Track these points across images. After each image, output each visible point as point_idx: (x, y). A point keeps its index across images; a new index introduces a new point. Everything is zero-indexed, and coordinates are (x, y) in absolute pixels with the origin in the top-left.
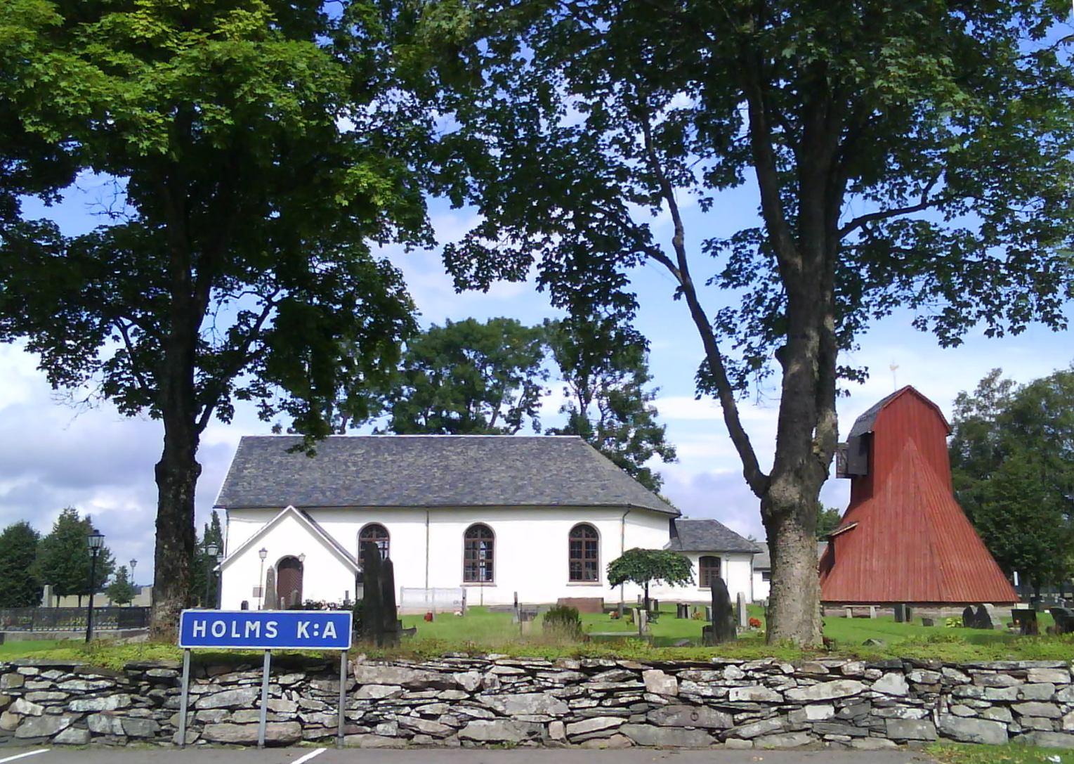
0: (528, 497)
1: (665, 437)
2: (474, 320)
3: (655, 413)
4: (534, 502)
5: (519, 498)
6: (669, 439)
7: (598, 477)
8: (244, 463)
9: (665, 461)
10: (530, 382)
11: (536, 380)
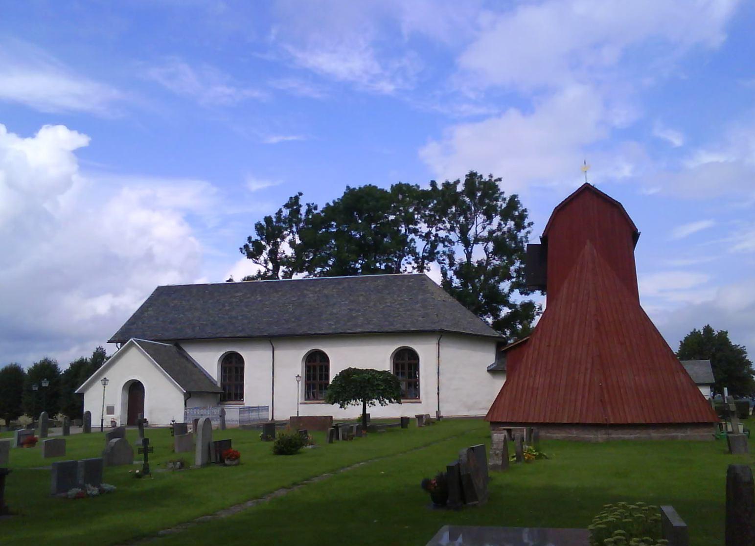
4: (359, 330)
10: (436, 235)
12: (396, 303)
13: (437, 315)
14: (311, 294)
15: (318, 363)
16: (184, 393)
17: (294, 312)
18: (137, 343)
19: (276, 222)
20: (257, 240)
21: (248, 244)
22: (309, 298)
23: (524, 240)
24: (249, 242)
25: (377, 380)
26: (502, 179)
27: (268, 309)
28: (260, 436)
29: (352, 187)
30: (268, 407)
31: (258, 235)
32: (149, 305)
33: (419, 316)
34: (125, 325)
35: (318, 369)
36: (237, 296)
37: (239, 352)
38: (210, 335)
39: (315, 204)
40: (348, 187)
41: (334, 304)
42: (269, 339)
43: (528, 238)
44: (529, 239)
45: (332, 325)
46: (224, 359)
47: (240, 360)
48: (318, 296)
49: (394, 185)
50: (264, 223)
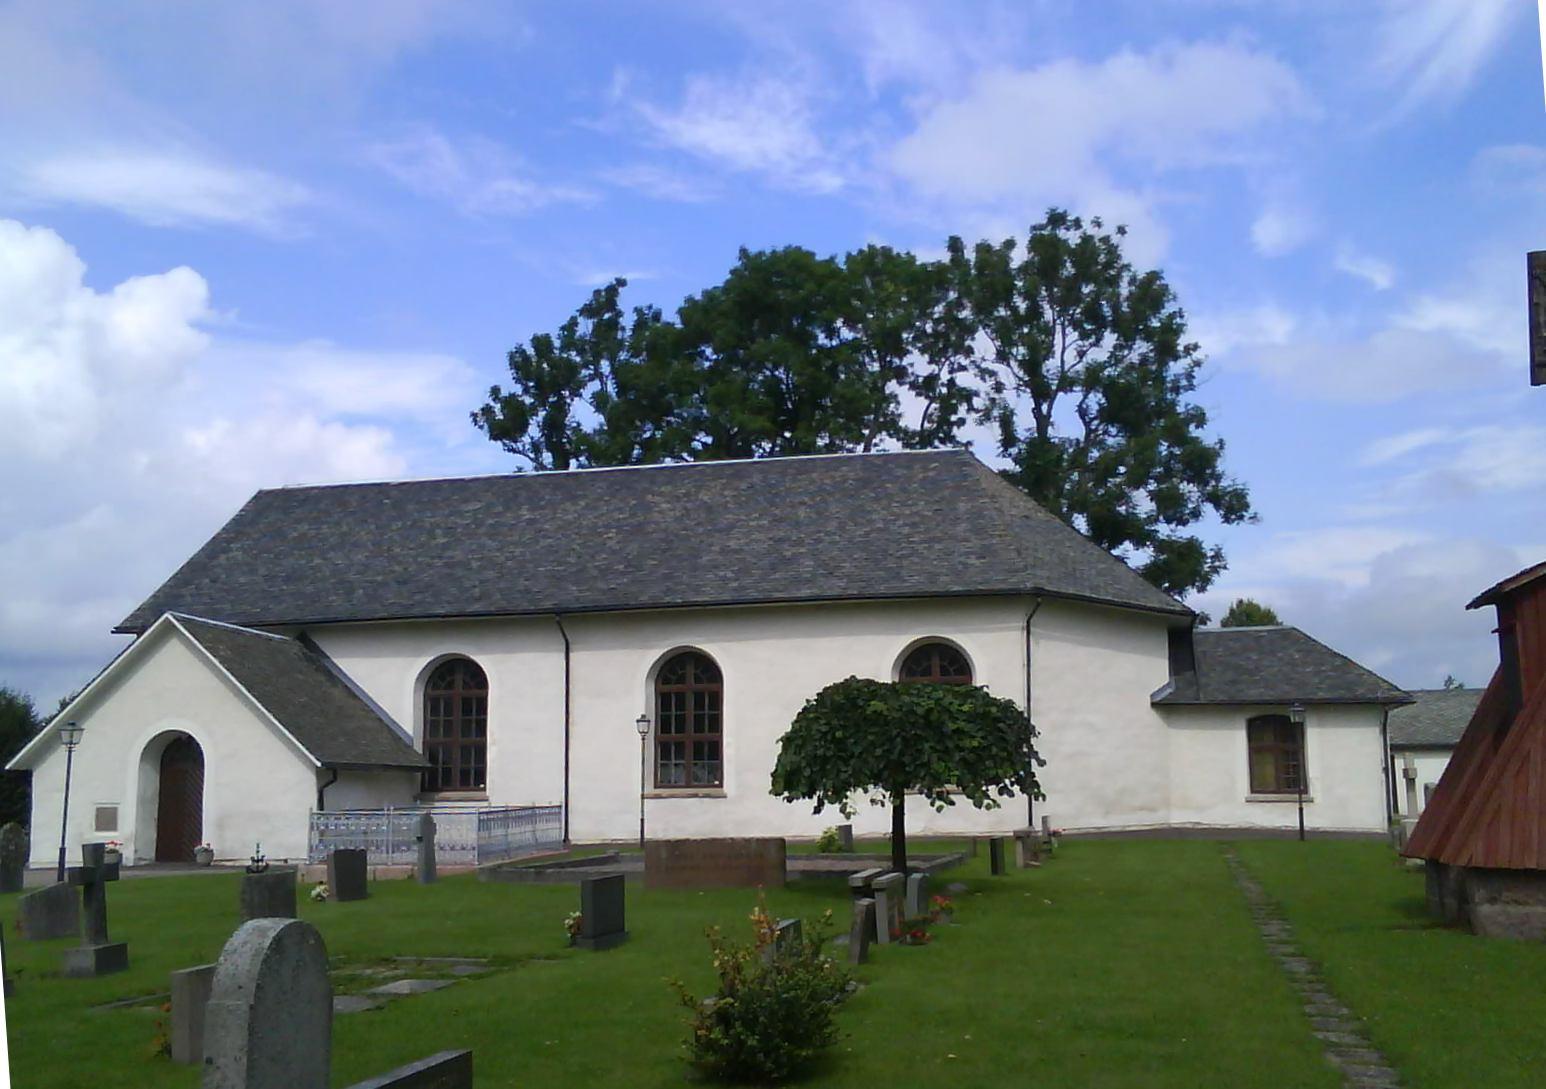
0: (798, 581)
1: (1221, 465)
2: (798, 249)
3: (1200, 418)
4: (805, 592)
5: (777, 585)
6: (1232, 470)
7: (978, 531)
9: (1227, 520)
10: (951, 383)
11: (965, 380)
14: (669, 502)
16: (317, 767)
19: (563, 349)
20: (513, 396)
21: (492, 404)
22: (660, 512)
23: (1184, 382)
24: (494, 400)
25: (955, 719)
27: (550, 540)
28: (571, 927)
29: (753, 250)
31: (517, 380)
32: (232, 535)
33: (967, 554)
34: (165, 586)
37: (472, 657)
38: (394, 611)
39: (654, 307)
40: (743, 252)
41: (731, 527)
42: (558, 618)
43: (1194, 377)
44: (1195, 382)
45: (729, 579)
46: (433, 673)
47: (477, 678)
48: (685, 509)
49: (854, 253)
50: (531, 351)
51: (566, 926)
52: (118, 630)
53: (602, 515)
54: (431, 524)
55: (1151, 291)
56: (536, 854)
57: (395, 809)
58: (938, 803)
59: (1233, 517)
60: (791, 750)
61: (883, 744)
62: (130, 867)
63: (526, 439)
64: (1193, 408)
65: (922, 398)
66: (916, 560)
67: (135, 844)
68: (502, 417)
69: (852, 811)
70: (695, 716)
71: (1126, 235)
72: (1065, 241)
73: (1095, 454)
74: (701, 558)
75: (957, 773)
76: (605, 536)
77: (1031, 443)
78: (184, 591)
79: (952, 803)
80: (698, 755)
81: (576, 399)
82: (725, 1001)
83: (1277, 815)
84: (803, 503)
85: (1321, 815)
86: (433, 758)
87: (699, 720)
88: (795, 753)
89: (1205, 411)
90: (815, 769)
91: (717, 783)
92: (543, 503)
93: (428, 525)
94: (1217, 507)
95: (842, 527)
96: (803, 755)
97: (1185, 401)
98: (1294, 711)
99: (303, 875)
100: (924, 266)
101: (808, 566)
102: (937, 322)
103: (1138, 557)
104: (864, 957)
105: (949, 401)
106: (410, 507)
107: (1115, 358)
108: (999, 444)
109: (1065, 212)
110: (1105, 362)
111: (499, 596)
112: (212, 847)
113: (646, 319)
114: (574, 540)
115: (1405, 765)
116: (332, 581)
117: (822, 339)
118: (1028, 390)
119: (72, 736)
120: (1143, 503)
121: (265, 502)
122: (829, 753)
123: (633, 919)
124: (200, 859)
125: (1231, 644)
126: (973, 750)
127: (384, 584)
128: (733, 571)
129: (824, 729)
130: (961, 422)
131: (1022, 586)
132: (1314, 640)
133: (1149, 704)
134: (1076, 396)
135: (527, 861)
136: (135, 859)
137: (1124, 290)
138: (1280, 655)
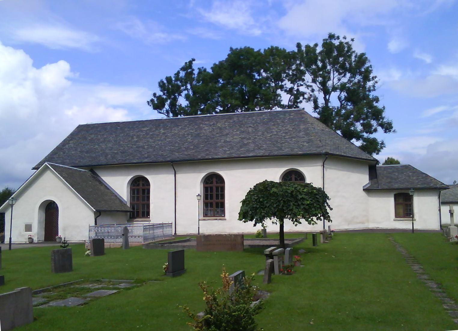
0: (248, 151)
1: (384, 115)
2: (249, 47)
4: (251, 155)
6: (387, 116)
7: (307, 134)
8: (71, 140)
9: (385, 132)
10: (298, 90)
11: (302, 89)
12: (282, 132)
13: (320, 141)
15: (214, 185)
16: (94, 211)
17: (192, 142)
18: (51, 166)
19: (175, 81)
20: (160, 96)
21: (154, 98)
23: (372, 88)
24: (154, 97)
26: (354, 39)
27: (170, 139)
28: (165, 268)
29: (234, 48)
30: (172, 223)
31: (161, 91)
32: (71, 139)
33: (304, 142)
35: (214, 189)
36: (144, 131)
37: (146, 176)
38: (120, 162)
39: (204, 68)
40: (231, 49)
41: (227, 134)
42: (172, 164)
43: (375, 87)
44: (376, 88)
45: (227, 150)
46: (133, 182)
47: (147, 183)
49: (267, 49)
50: (165, 82)
51: (163, 268)
52: (34, 169)
53: (186, 131)
54: (132, 134)
55: (362, 59)
56: (164, 239)
57: (116, 225)
58: (296, 223)
59: (388, 131)
60: (245, 206)
61: (276, 203)
62: (37, 243)
63: (164, 109)
64: (375, 97)
65: (289, 95)
66: (286, 144)
67: (37, 236)
68: (156, 102)
69: (266, 226)
70: (216, 194)
71: (354, 41)
72: (334, 44)
73: (343, 111)
74: (218, 144)
75: (302, 213)
76: (187, 138)
77: (323, 108)
78: (54, 156)
79: (301, 223)
80: (217, 206)
81: (180, 97)
82: (207, 316)
83: (404, 225)
84: (250, 127)
85: (419, 225)
86: (133, 208)
87: (217, 196)
88: (246, 206)
89: (379, 97)
90: (253, 212)
91: (223, 215)
92: (168, 128)
93: (131, 135)
94: (382, 128)
95: (263, 134)
96: (249, 207)
97: (372, 95)
98: (411, 191)
99: (87, 246)
100: (289, 52)
101: (252, 146)
102: (293, 71)
103: (358, 143)
104: (270, 281)
105: (297, 96)
106: (126, 129)
107: (350, 81)
108: (313, 108)
109: (334, 34)
110: (347, 82)
111: (153, 157)
112: (61, 237)
113: (202, 71)
114: (177, 139)
115: (450, 209)
116: (101, 152)
117: (257, 76)
118: (322, 91)
119: (12, 202)
120: (359, 127)
121: (81, 128)
122: (258, 206)
123: (188, 264)
124: (58, 240)
125: (389, 170)
126: (308, 205)
127: (117, 153)
128: (228, 148)
129: (256, 198)
130: (301, 102)
131: (321, 152)
132: (416, 169)
133: (362, 190)
134: (338, 93)
135: (161, 241)
136: (38, 241)
137: (353, 59)
138: (405, 173)
